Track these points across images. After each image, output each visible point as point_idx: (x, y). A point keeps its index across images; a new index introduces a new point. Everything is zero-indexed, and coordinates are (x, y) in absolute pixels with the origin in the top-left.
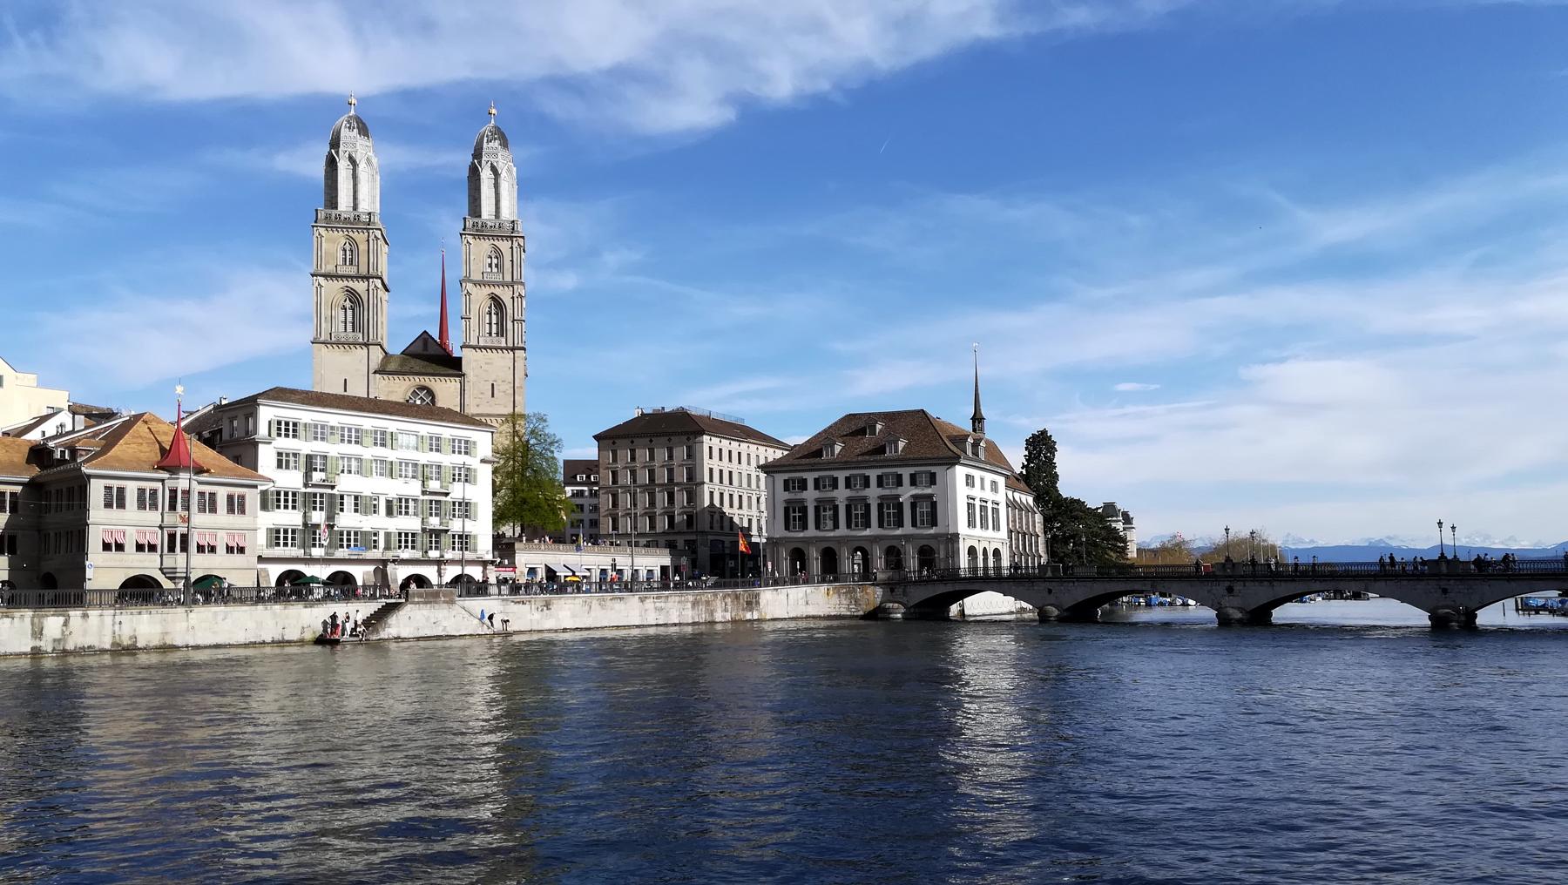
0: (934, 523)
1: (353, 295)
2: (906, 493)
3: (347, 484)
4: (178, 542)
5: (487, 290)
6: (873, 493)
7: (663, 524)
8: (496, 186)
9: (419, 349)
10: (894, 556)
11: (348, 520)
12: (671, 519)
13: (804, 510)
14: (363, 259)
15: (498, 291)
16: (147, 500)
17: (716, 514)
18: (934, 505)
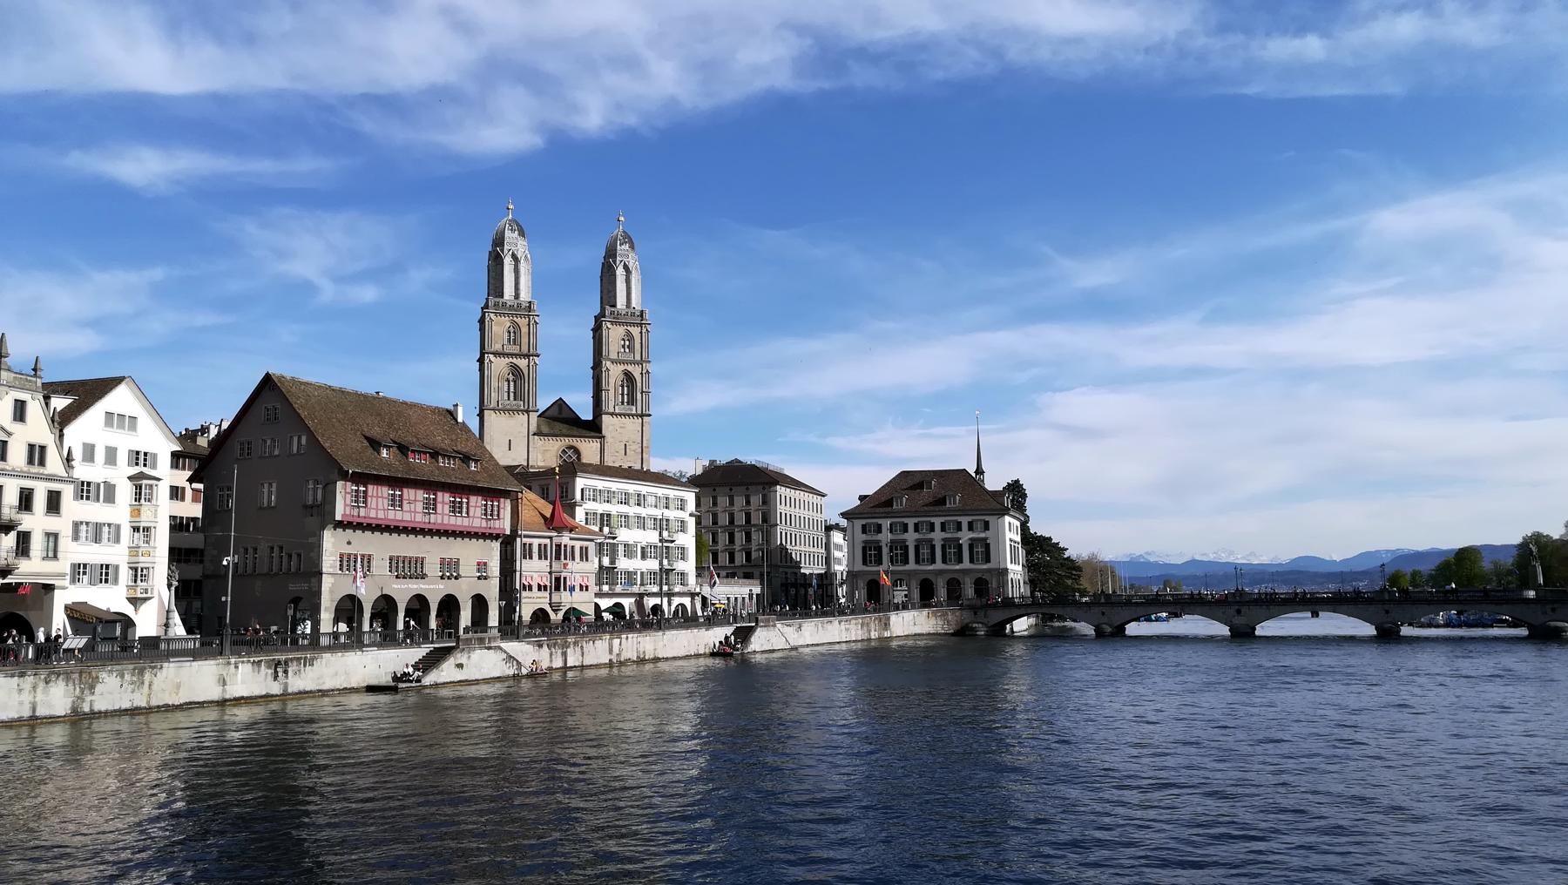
0: (988, 560)
1: (516, 371)
2: (965, 536)
3: (624, 535)
4: (558, 584)
5: (622, 367)
6: (938, 536)
7: (740, 559)
8: (628, 281)
9: (554, 412)
10: (954, 587)
11: (623, 564)
12: (748, 555)
13: (879, 549)
14: (525, 340)
15: (630, 368)
16: (543, 554)
17: (783, 549)
18: (987, 546)
